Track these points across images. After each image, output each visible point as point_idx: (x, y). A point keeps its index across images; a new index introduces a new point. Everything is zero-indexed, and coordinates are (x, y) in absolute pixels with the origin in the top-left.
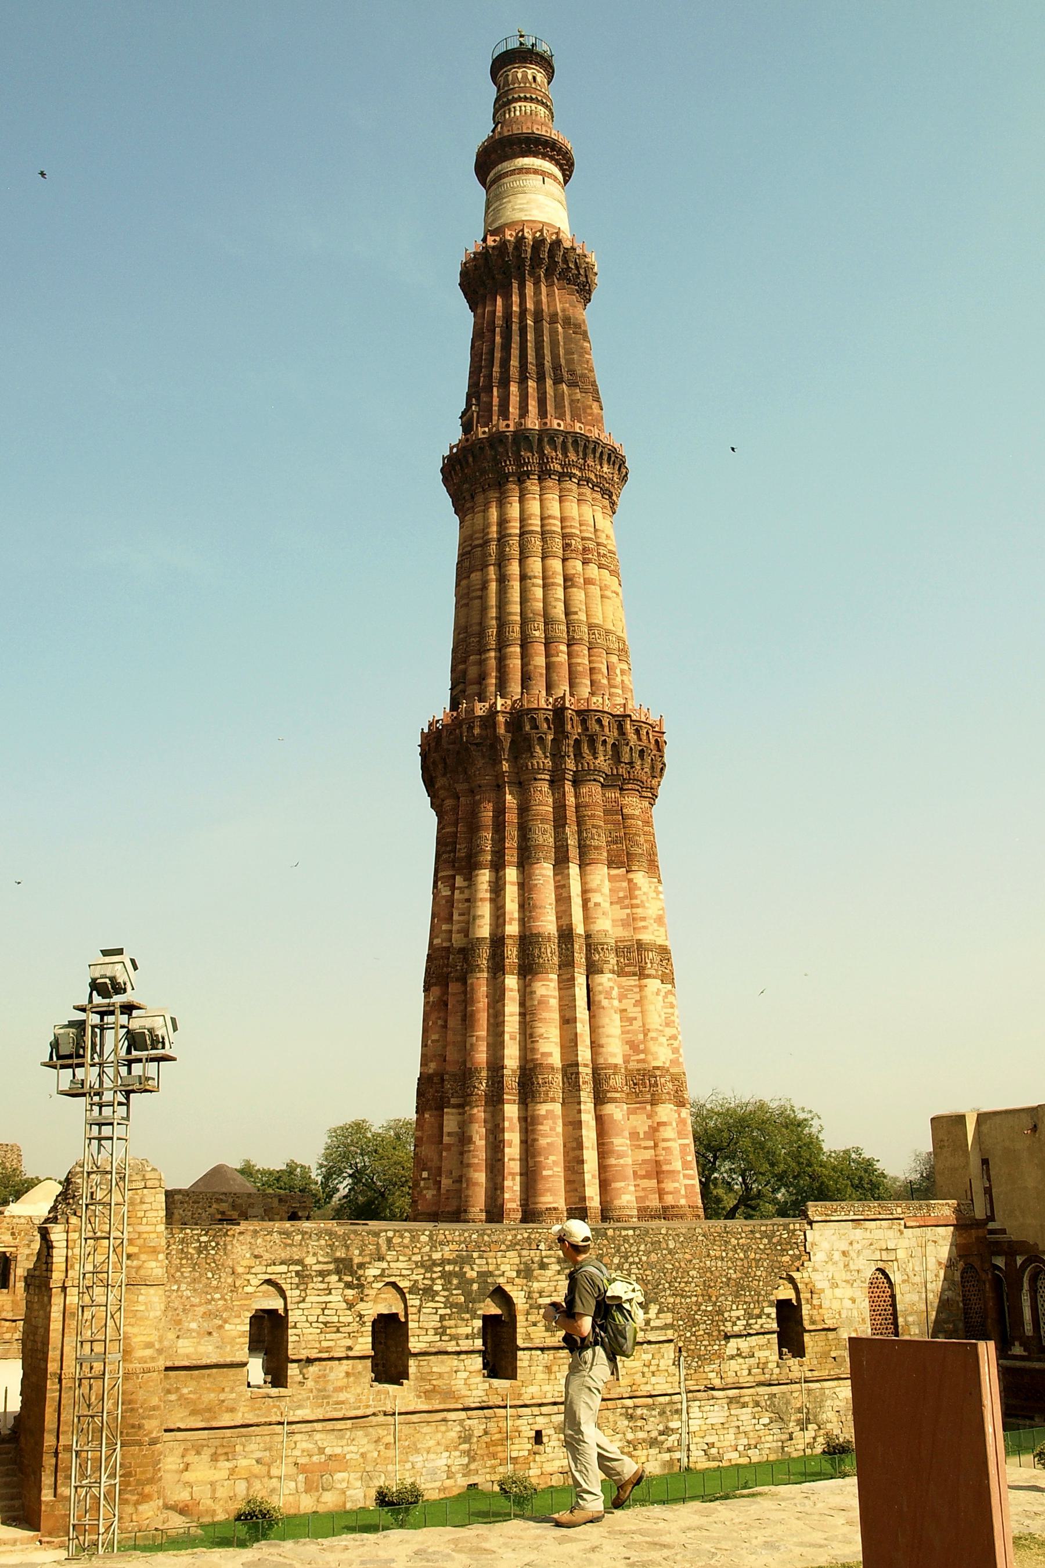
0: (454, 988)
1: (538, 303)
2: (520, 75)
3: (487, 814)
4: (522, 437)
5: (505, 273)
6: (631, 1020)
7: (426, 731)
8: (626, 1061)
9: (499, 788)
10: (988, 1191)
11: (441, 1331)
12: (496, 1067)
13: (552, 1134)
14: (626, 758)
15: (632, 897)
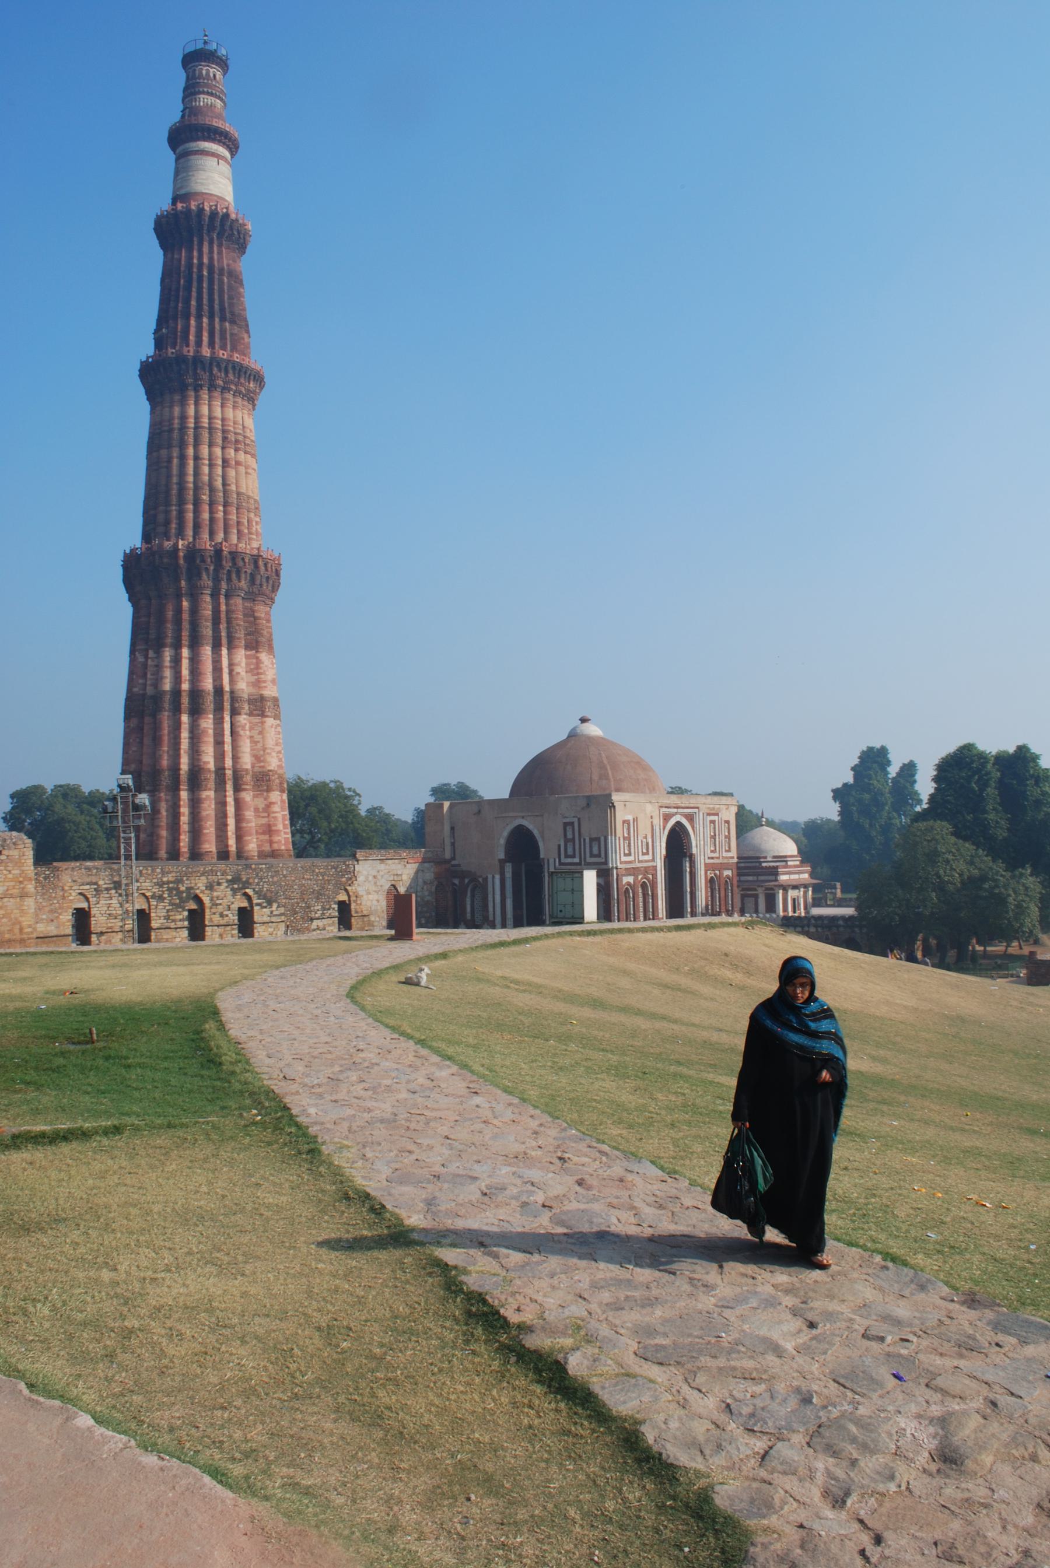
0: (147, 719)
1: (211, 259)
2: (204, 72)
3: (170, 614)
4: (198, 360)
5: (190, 235)
6: (256, 743)
7: (128, 551)
8: (253, 767)
9: (179, 597)
10: (453, 844)
11: (167, 918)
12: (175, 768)
13: (209, 809)
14: (258, 582)
15: (258, 667)
